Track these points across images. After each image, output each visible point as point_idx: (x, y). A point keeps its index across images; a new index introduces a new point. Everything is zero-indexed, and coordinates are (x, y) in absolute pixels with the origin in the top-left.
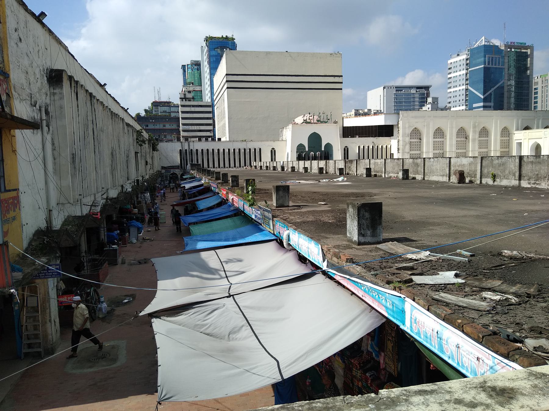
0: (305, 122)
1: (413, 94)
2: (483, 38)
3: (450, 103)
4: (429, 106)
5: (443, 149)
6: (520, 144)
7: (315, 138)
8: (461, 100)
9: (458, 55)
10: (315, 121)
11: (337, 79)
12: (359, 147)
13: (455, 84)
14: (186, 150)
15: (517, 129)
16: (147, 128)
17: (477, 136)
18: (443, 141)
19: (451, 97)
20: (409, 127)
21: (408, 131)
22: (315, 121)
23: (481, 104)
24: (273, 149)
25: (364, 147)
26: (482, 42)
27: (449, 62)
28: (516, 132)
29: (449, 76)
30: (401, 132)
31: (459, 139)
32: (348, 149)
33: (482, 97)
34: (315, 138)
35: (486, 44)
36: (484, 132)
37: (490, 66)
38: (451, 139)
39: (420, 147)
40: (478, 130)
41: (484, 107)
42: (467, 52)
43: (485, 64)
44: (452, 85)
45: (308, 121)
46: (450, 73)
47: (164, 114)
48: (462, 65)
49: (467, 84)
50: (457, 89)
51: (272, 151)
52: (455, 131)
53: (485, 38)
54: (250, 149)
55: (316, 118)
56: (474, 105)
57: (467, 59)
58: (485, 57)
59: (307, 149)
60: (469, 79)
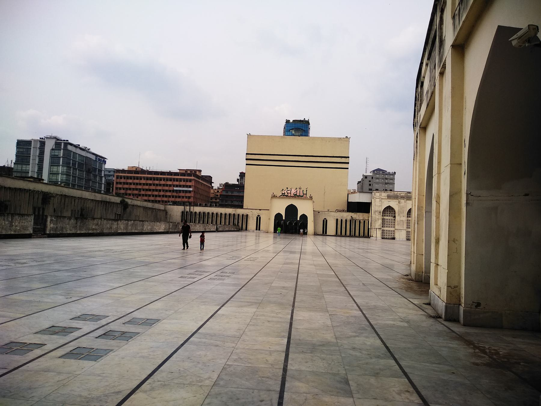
7: (291, 210)
10: (292, 195)
11: (343, 160)
14: (187, 212)
22: (292, 195)
34: (291, 210)
39: (394, 225)
45: (286, 194)
55: (293, 191)
59: (284, 218)
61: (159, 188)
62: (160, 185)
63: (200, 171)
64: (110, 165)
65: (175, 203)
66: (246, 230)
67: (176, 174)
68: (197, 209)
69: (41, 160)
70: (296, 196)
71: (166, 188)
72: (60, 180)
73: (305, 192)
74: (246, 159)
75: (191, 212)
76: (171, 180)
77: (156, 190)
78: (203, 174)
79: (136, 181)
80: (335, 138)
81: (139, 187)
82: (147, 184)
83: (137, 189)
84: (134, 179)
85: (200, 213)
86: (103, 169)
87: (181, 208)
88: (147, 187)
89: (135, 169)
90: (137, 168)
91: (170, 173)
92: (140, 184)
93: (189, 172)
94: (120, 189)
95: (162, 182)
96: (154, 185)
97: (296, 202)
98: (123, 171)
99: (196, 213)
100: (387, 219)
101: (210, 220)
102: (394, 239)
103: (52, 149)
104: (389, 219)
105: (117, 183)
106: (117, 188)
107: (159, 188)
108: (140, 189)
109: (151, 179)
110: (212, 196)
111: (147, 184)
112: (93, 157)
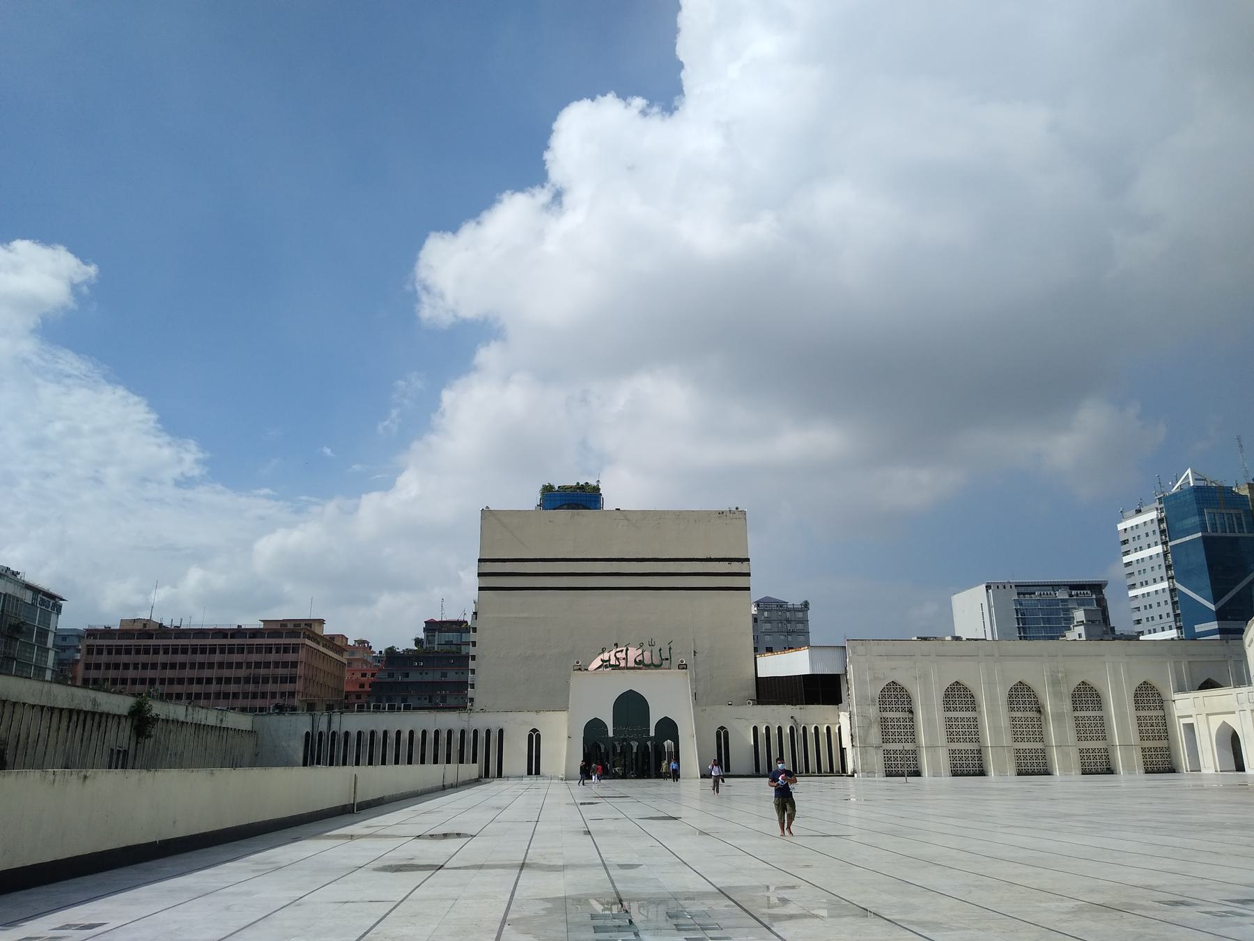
0: (606, 664)
1: (1063, 600)
2: (1189, 471)
3: (1139, 622)
4: (1081, 630)
5: (978, 741)
6: (1190, 728)
7: (631, 706)
8: (1164, 616)
9: (1139, 511)
11: (735, 567)
12: (755, 729)
13: (1143, 578)
15: (1181, 689)
16: (406, 680)
17: (1067, 705)
18: (975, 719)
19: (1138, 609)
20: (875, 679)
21: (875, 690)
23: (1214, 625)
24: (535, 730)
25: (767, 729)
26: (1188, 477)
27: (1121, 527)
28: (1176, 696)
29: (1126, 559)
30: (853, 691)
31: (1019, 714)
32: (726, 734)
33: (1212, 607)
34: (631, 706)
35: (1201, 483)
36: (1086, 697)
37: (1219, 534)
38: (993, 712)
39: (913, 734)
40: (1067, 690)
41: (1221, 631)
42: (1157, 504)
43: (1204, 529)
44: (1137, 579)
45: (612, 662)
46: (1127, 553)
47: (447, 647)
48: (1151, 534)
49: (1172, 578)
50: (1151, 588)
51: (530, 737)
52: (1002, 694)
53: (1193, 472)
54: (476, 732)
55: (633, 653)
56: (1199, 628)
57: (1160, 521)
58: (1201, 513)
59: (611, 734)
60: (1175, 565)
61: (206, 673)
63: (321, 622)
64: (70, 619)
65: (280, 709)
66: (500, 775)
67: (255, 633)
68: (353, 723)
70: (640, 664)
71: (226, 673)
73: (665, 655)
74: (480, 575)
75: (334, 733)
76: (241, 650)
77: (200, 681)
78: (328, 630)
79: (142, 658)
80: (709, 513)
81: (150, 674)
84: (138, 652)
85: (359, 733)
86: (52, 628)
87: (301, 724)
88: (169, 673)
89: (139, 626)
90: (146, 623)
91: (239, 632)
93: (290, 626)
97: (641, 683)
98: (107, 633)
99: (347, 734)
100: (892, 719)
101: (391, 754)
102: (917, 774)
104: (898, 719)
107: (206, 673)
109: (184, 650)
110: (347, 688)
111: (173, 666)
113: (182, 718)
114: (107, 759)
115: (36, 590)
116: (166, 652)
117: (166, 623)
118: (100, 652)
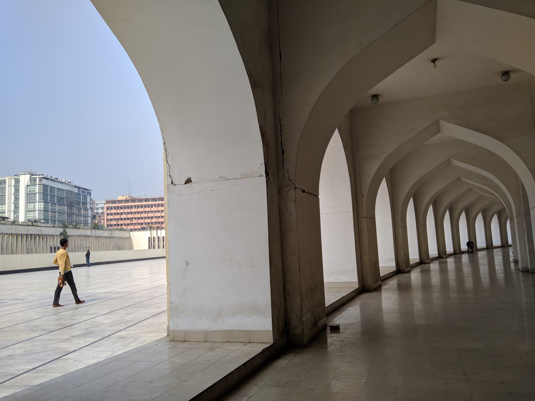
62: (152, 212)
69: (17, 199)
72: (37, 217)
77: (149, 218)
82: (138, 213)
83: (128, 219)
84: (125, 208)
86: (88, 200)
87: (146, 234)
88: (139, 216)
92: (132, 213)
94: (111, 220)
95: (154, 209)
96: (145, 212)
98: (114, 202)
103: (28, 186)
105: (108, 214)
106: (108, 220)
108: (132, 218)
111: (138, 213)
112: (76, 190)
113: (89, 234)
114: (49, 250)
115: (79, 188)
116: (135, 207)
117: (134, 197)
118: (111, 208)
